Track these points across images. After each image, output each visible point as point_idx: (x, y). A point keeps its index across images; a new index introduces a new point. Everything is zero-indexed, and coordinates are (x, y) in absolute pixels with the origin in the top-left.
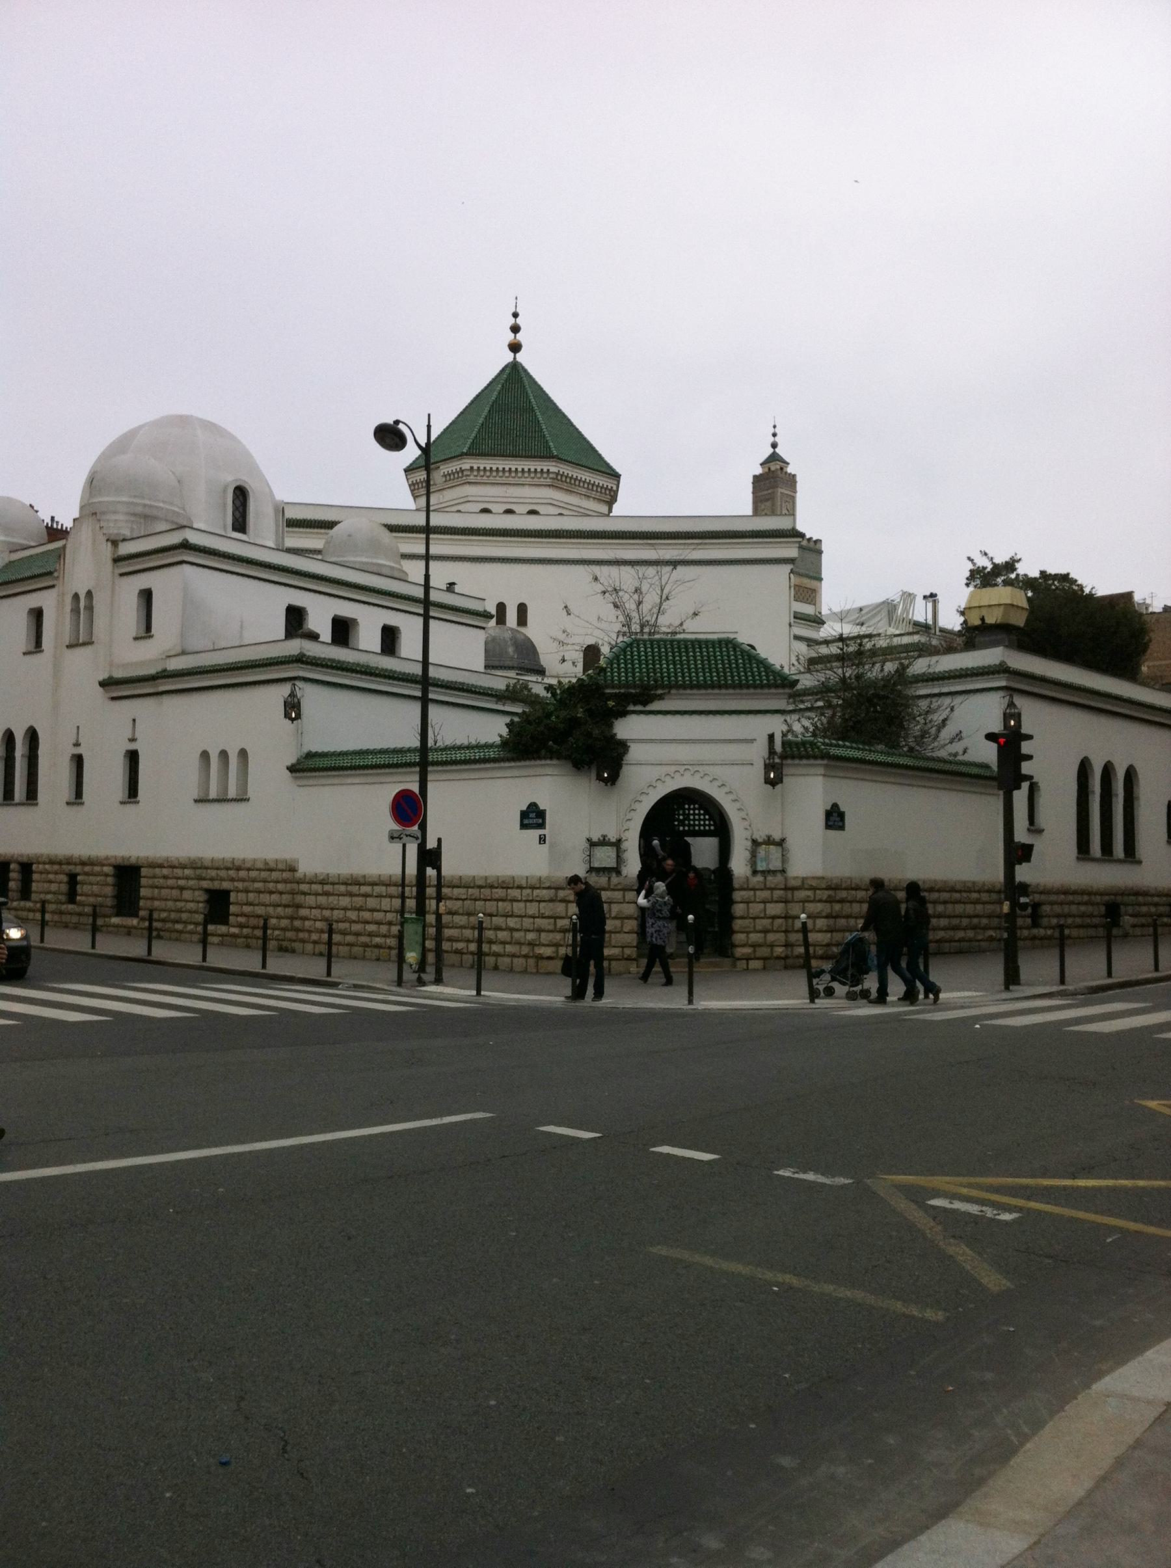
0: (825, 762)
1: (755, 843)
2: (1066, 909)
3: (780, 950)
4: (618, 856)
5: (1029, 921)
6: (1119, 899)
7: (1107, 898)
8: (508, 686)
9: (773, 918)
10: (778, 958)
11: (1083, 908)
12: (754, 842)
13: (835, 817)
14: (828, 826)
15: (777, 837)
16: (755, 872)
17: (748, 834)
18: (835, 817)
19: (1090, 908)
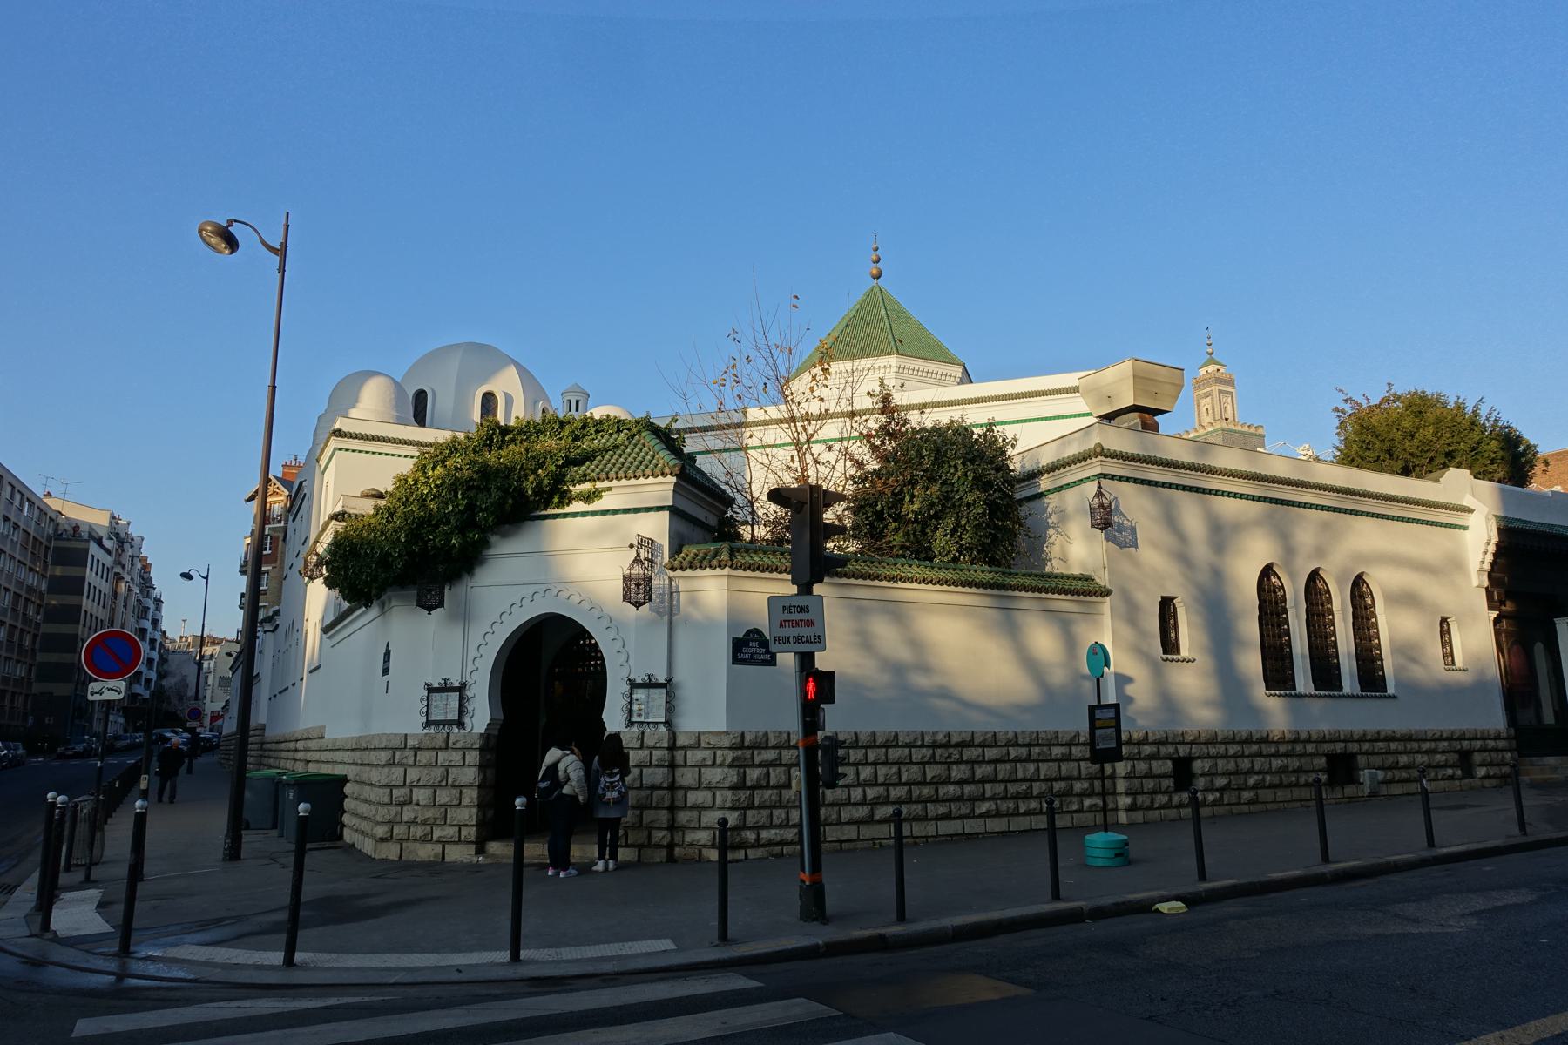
0: (727, 571)
1: (634, 685)
2: (1245, 764)
3: (660, 834)
4: (461, 705)
5: (1168, 783)
6: (1353, 747)
7: (1327, 747)
8: (377, 508)
9: (653, 788)
10: (658, 846)
11: (1277, 763)
12: (634, 685)
13: (754, 647)
14: (736, 660)
15: (661, 678)
16: (630, 724)
17: (624, 673)
18: (754, 647)
19: (1294, 763)
